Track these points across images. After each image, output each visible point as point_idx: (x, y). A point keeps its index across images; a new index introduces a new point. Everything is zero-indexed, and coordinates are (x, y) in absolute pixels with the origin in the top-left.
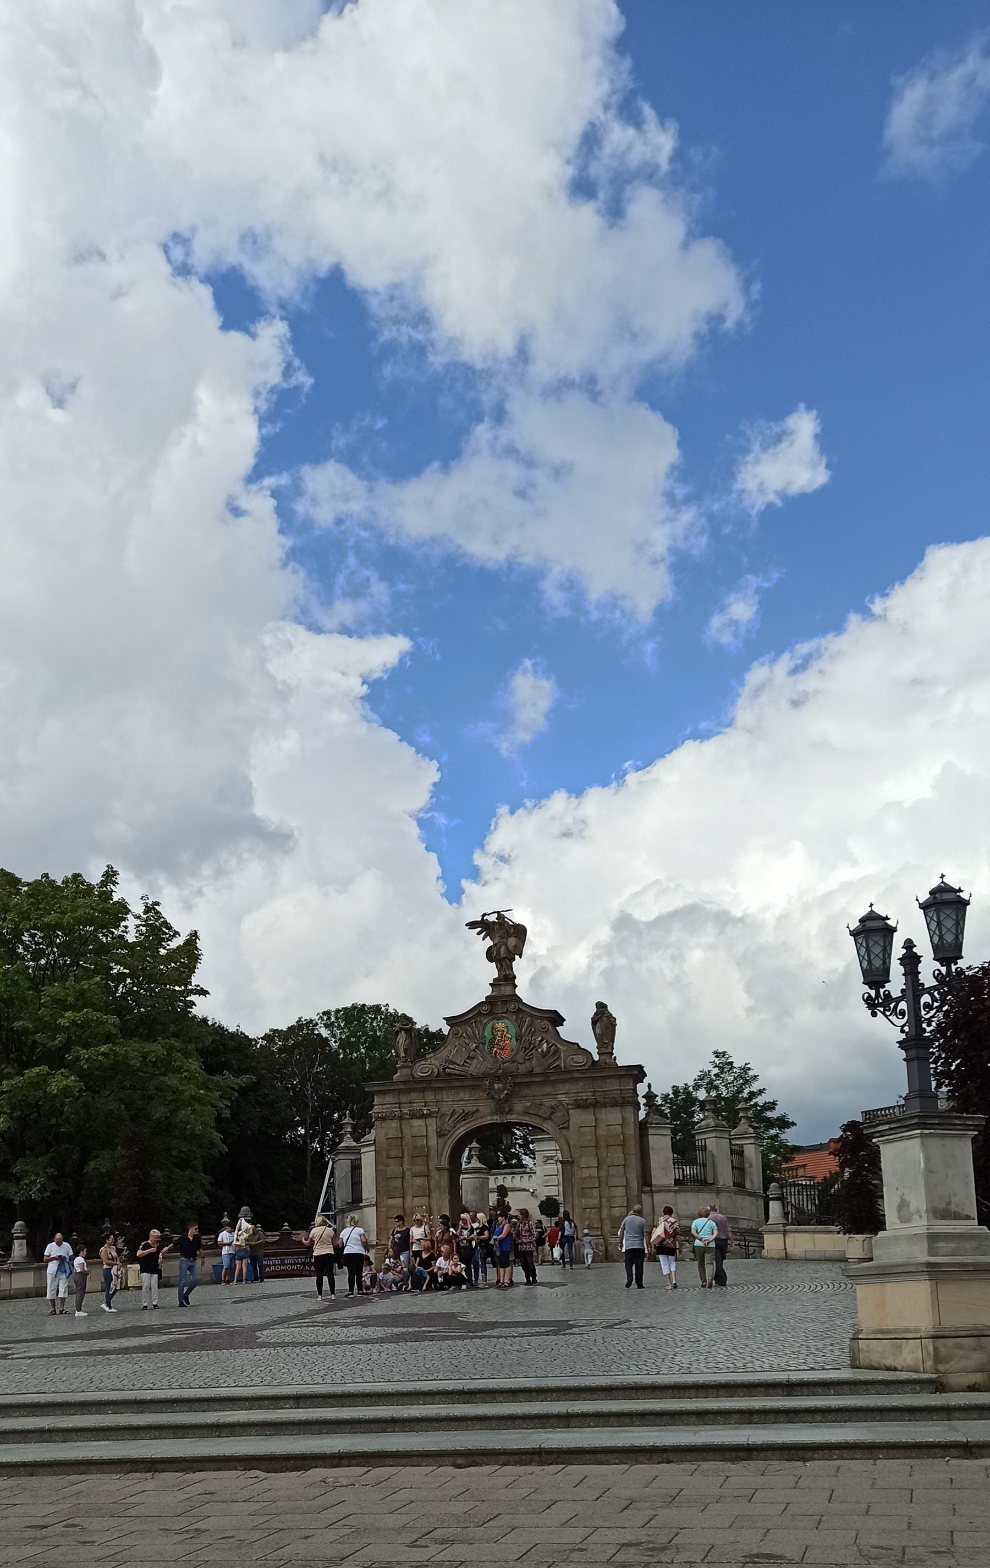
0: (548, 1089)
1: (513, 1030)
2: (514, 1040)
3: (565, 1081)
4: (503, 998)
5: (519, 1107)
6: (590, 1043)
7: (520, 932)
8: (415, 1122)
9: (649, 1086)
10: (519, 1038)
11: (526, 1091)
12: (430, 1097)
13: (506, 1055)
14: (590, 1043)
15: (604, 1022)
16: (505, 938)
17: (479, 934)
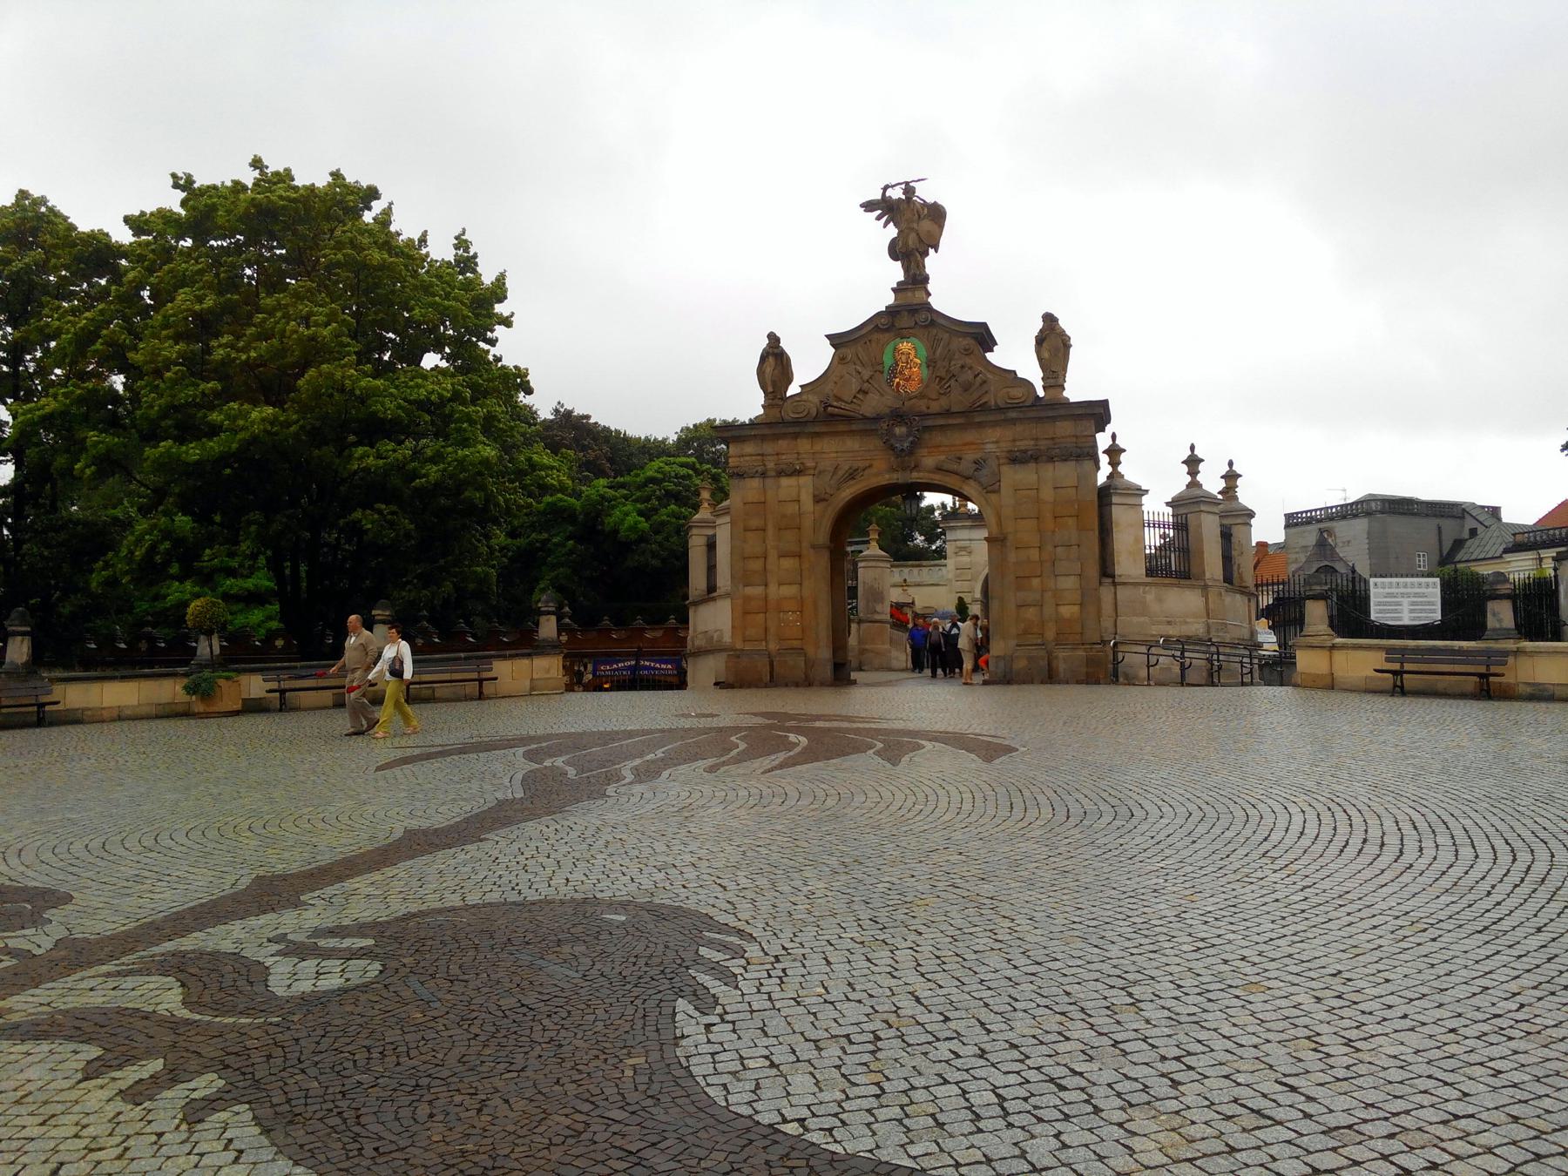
0: (970, 436)
1: (923, 352)
2: (924, 367)
3: (995, 424)
4: (911, 310)
5: (929, 461)
6: (1031, 371)
7: (937, 214)
8: (785, 481)
9: (1114, 437)
10: (931, 363)
11: (938, 438)
12: (804, 445)
13: (913, 388)
14: (1031, 371)
15: (1053, 343)
16: (913, 225)
17: (879, 218)
